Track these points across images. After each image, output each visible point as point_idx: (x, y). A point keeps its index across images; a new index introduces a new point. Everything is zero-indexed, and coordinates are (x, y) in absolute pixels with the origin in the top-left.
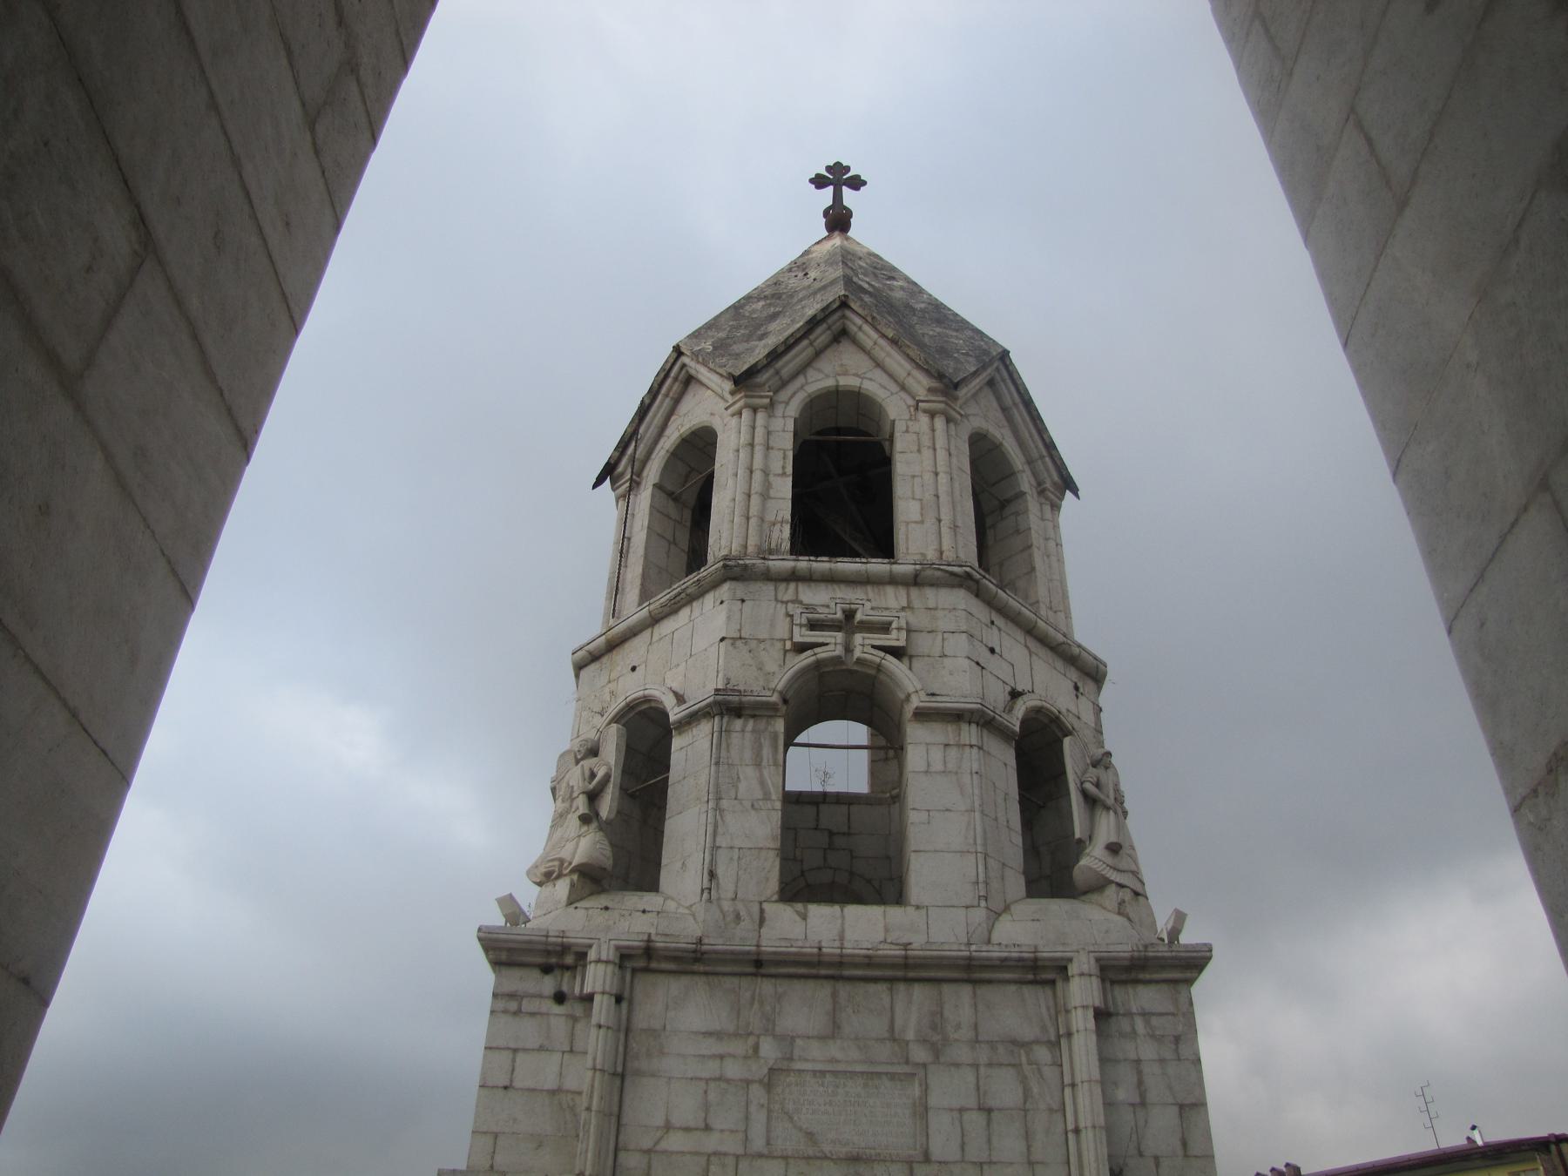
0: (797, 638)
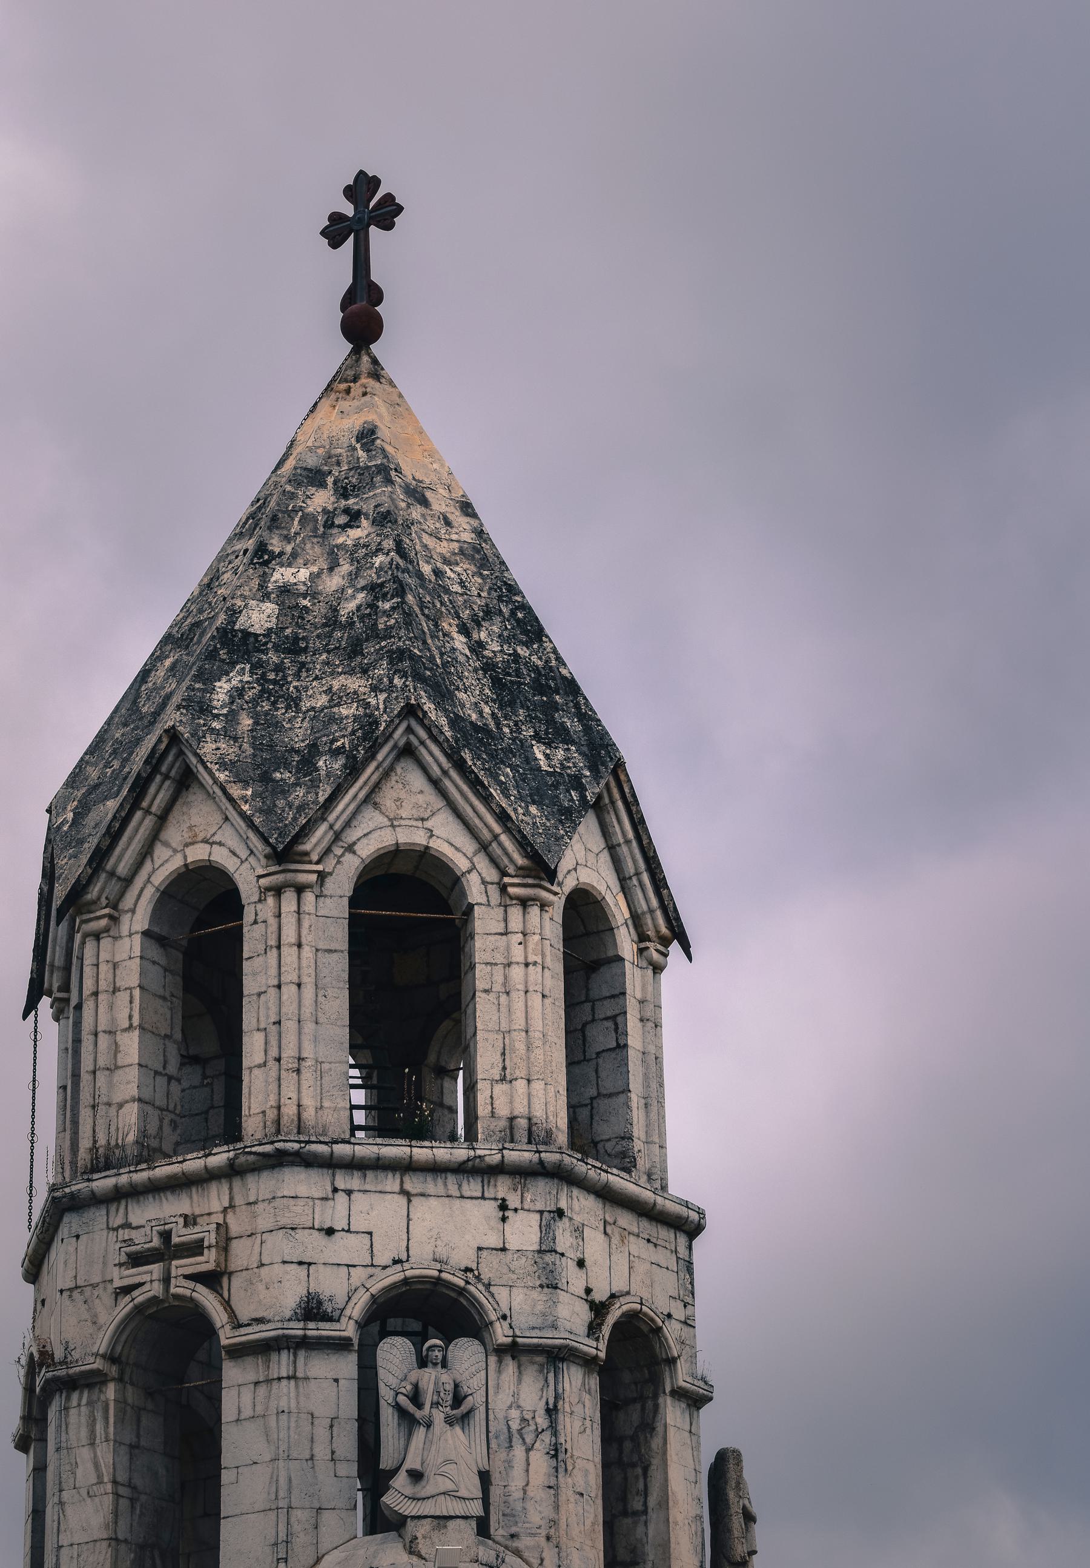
0: (118, 1283)
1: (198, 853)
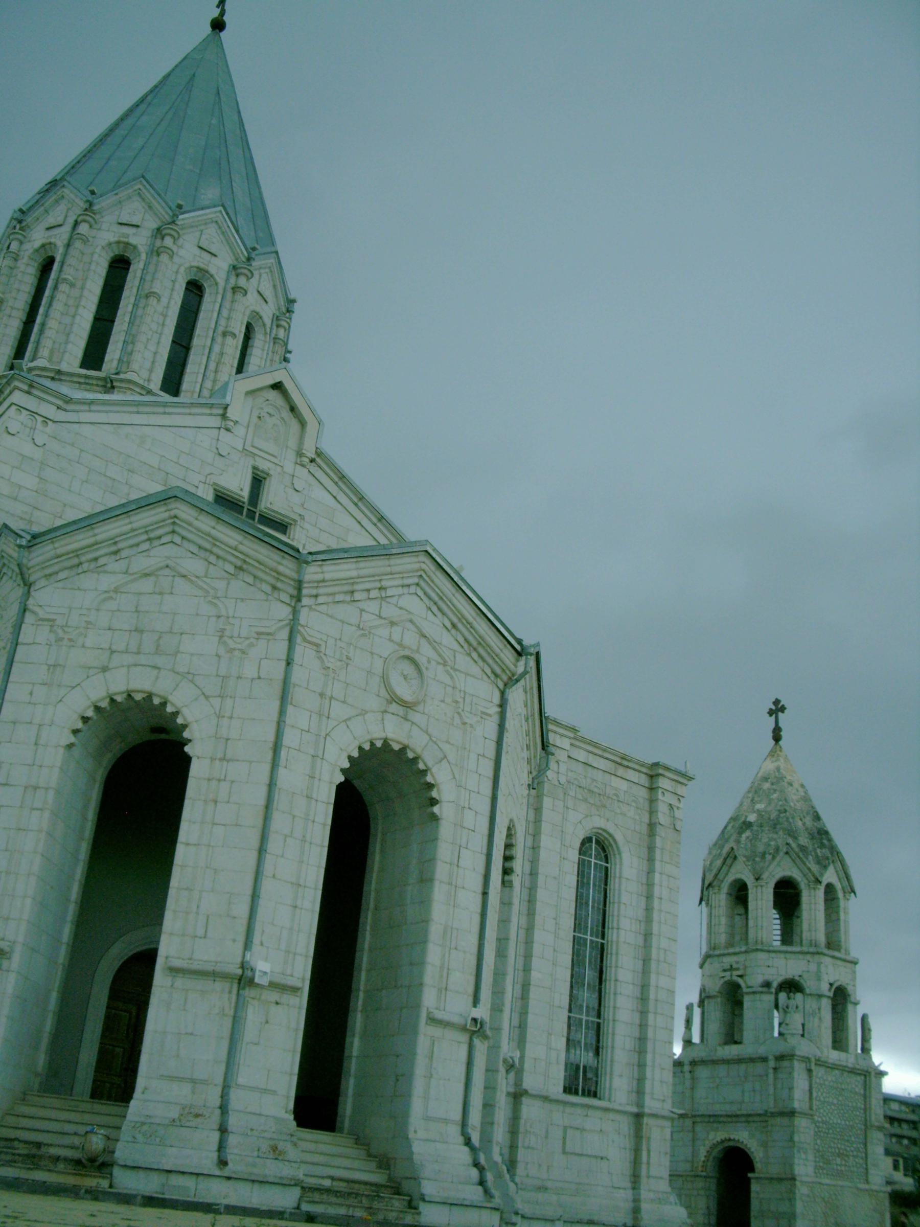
1: (739, 876)
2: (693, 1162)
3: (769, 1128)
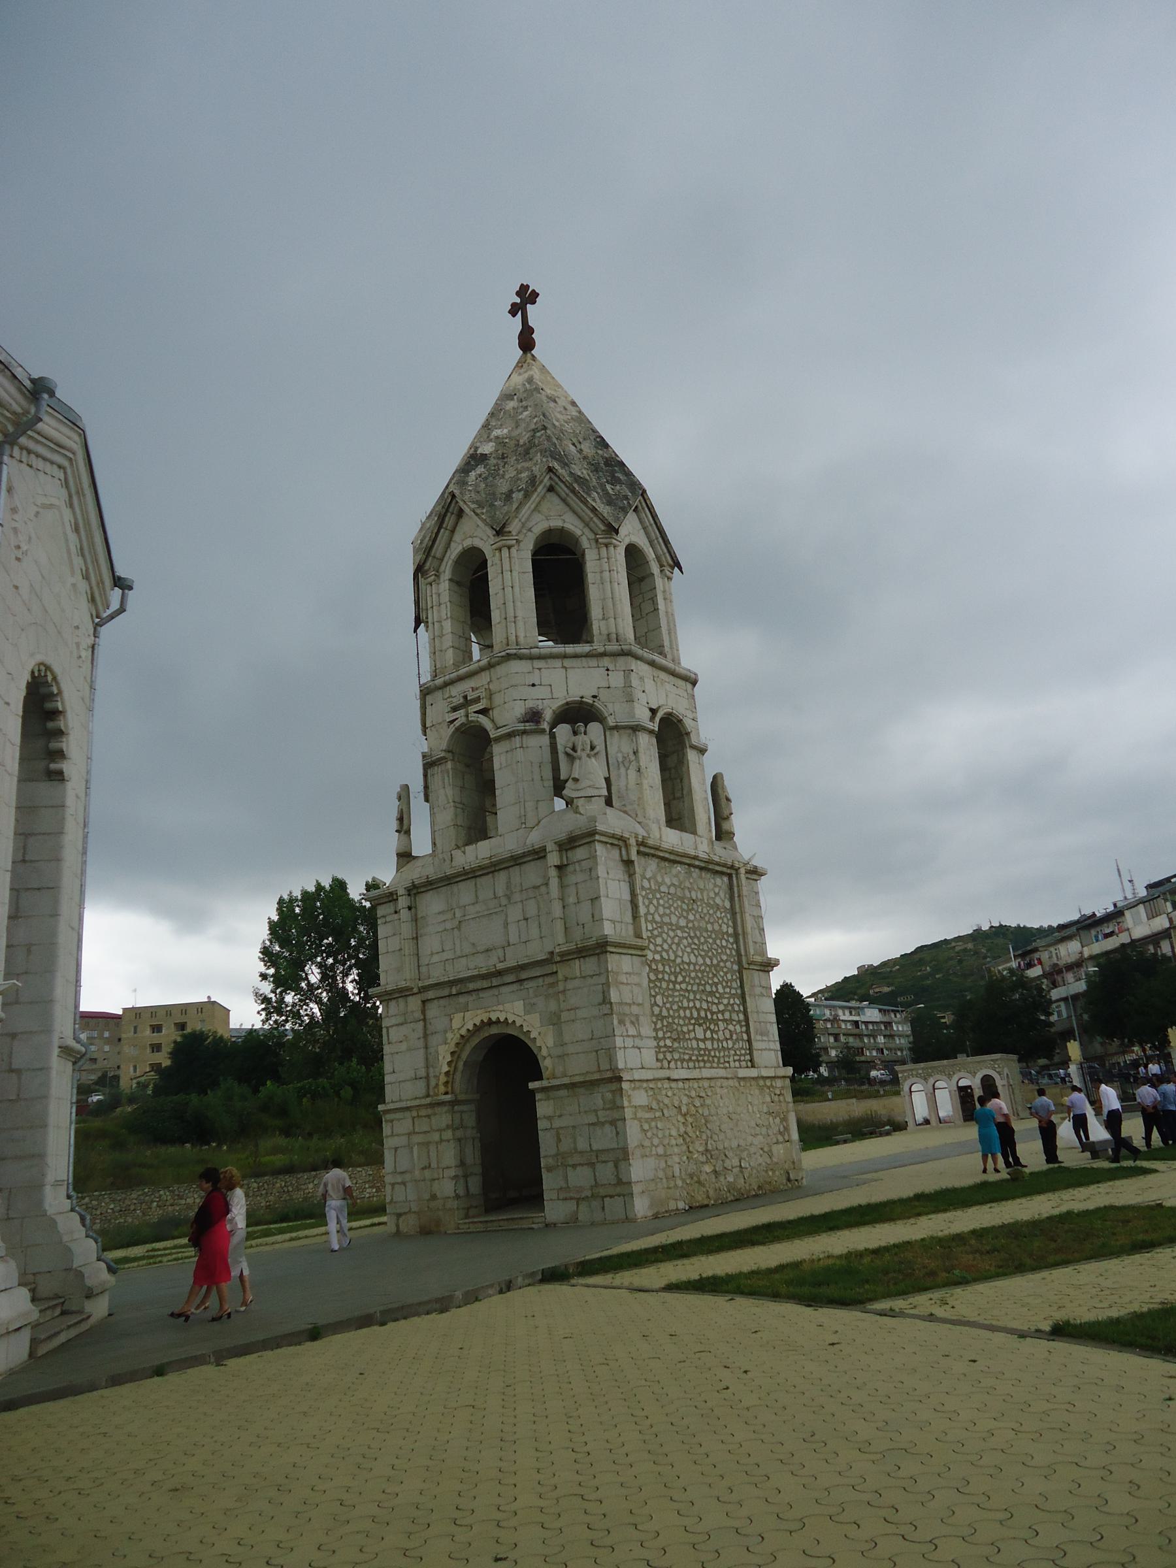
1: (468, 543)
2: (427, 1077)
3: (561, 987)
